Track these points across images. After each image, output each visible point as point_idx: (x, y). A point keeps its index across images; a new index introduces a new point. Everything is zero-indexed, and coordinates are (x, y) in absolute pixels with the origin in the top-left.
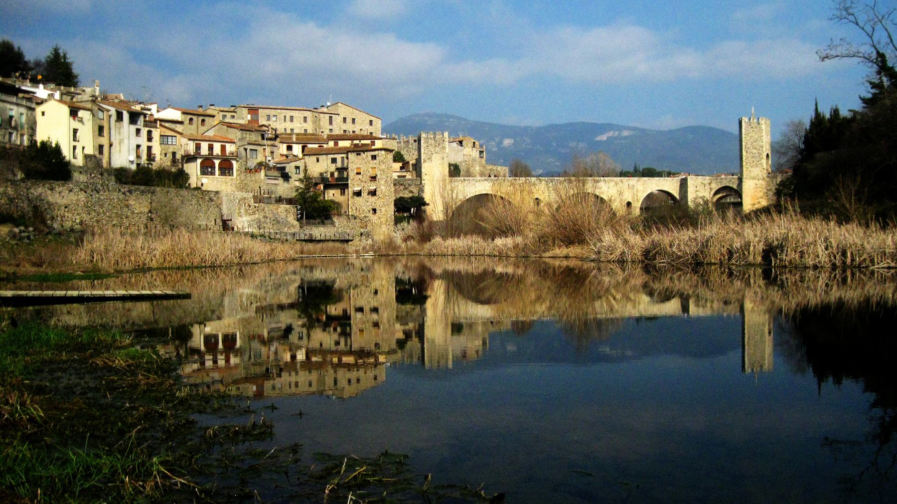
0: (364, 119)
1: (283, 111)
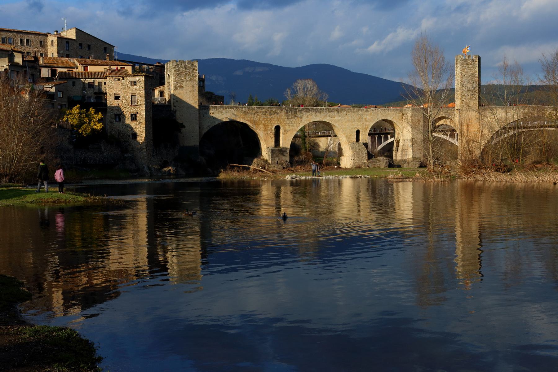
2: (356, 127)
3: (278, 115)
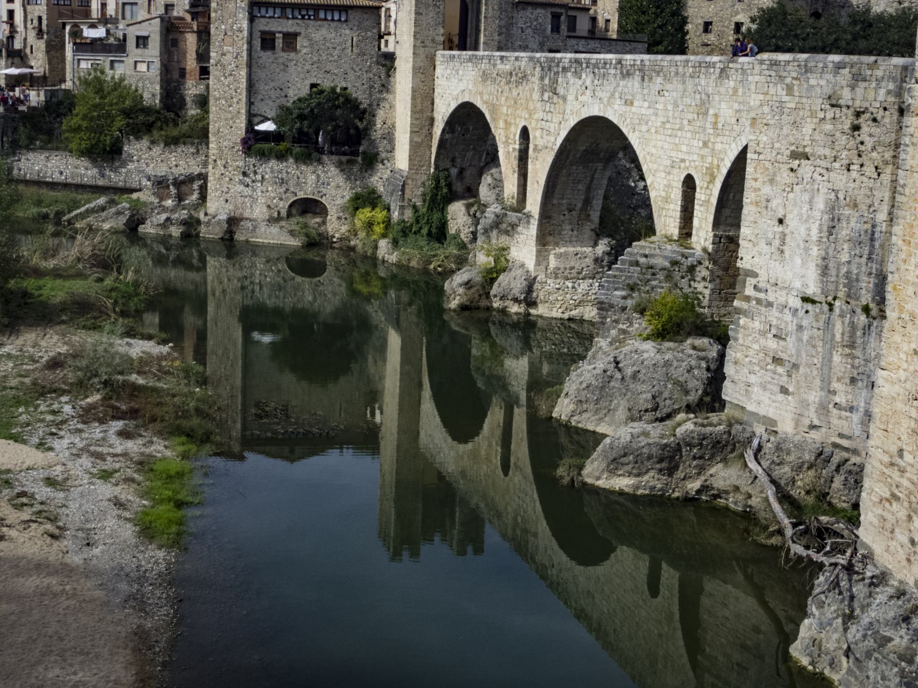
2: (683, 161)
3: (527, 88)
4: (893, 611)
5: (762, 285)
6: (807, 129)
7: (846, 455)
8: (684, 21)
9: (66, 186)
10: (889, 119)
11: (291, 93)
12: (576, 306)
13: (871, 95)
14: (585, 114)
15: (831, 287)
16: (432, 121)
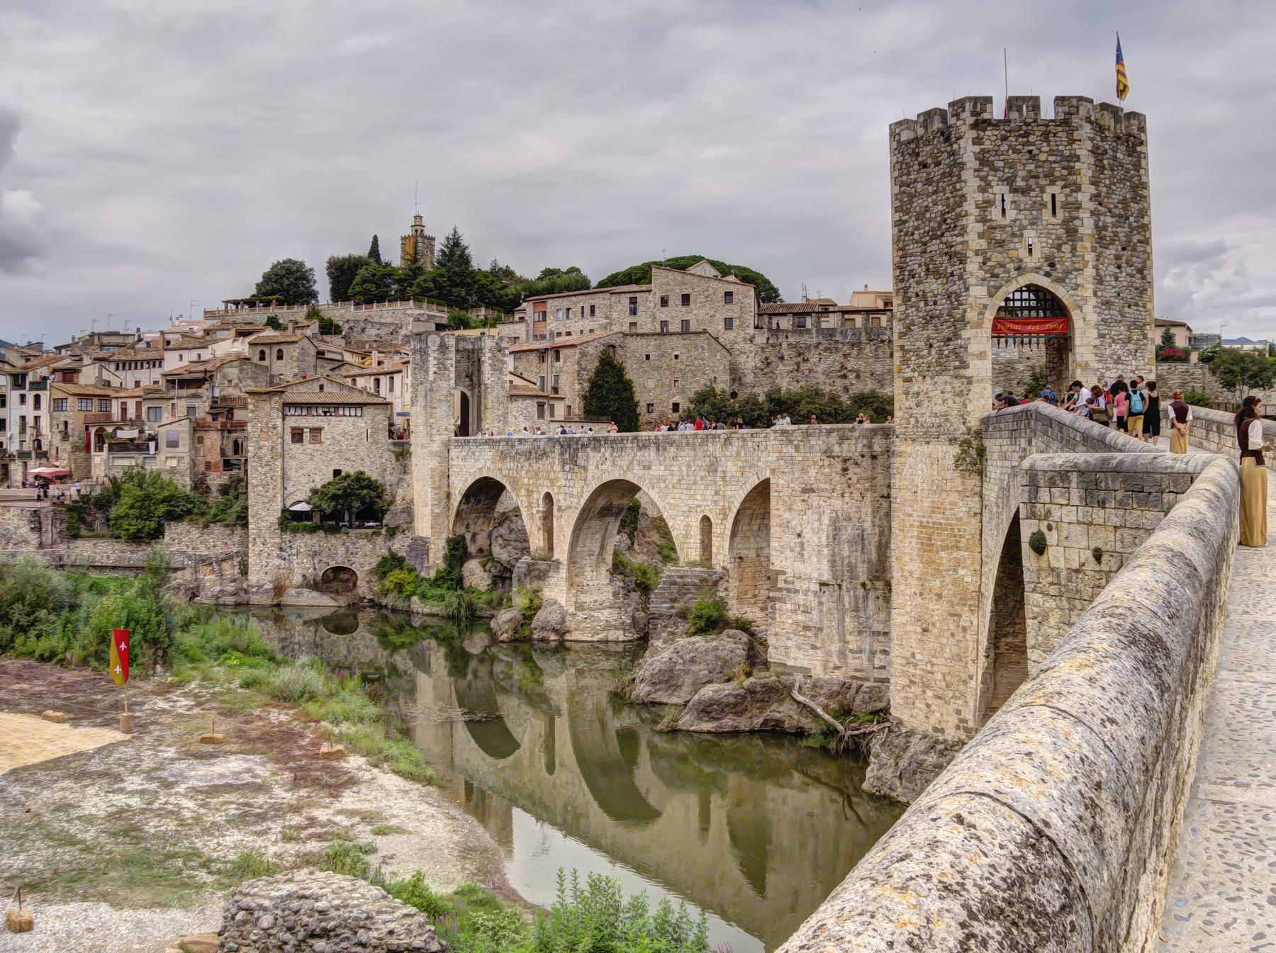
0: (711, 291)
1: (580, 298)
2: (699, 506)
4: (923, 746)
5: (790, 579)
6: (812, 472)
7: (860, 683)
8: (636, 405)
9: (114, 568)
10: (866, 462)
11: (317, 478)
12: (603, 630)
13: (853, 448)
14: (607, 478)
15: (839, 573)
16: (448, 495)
